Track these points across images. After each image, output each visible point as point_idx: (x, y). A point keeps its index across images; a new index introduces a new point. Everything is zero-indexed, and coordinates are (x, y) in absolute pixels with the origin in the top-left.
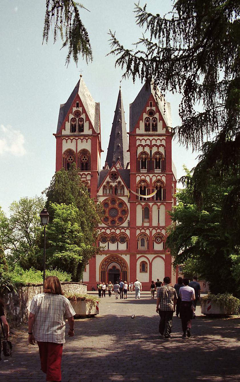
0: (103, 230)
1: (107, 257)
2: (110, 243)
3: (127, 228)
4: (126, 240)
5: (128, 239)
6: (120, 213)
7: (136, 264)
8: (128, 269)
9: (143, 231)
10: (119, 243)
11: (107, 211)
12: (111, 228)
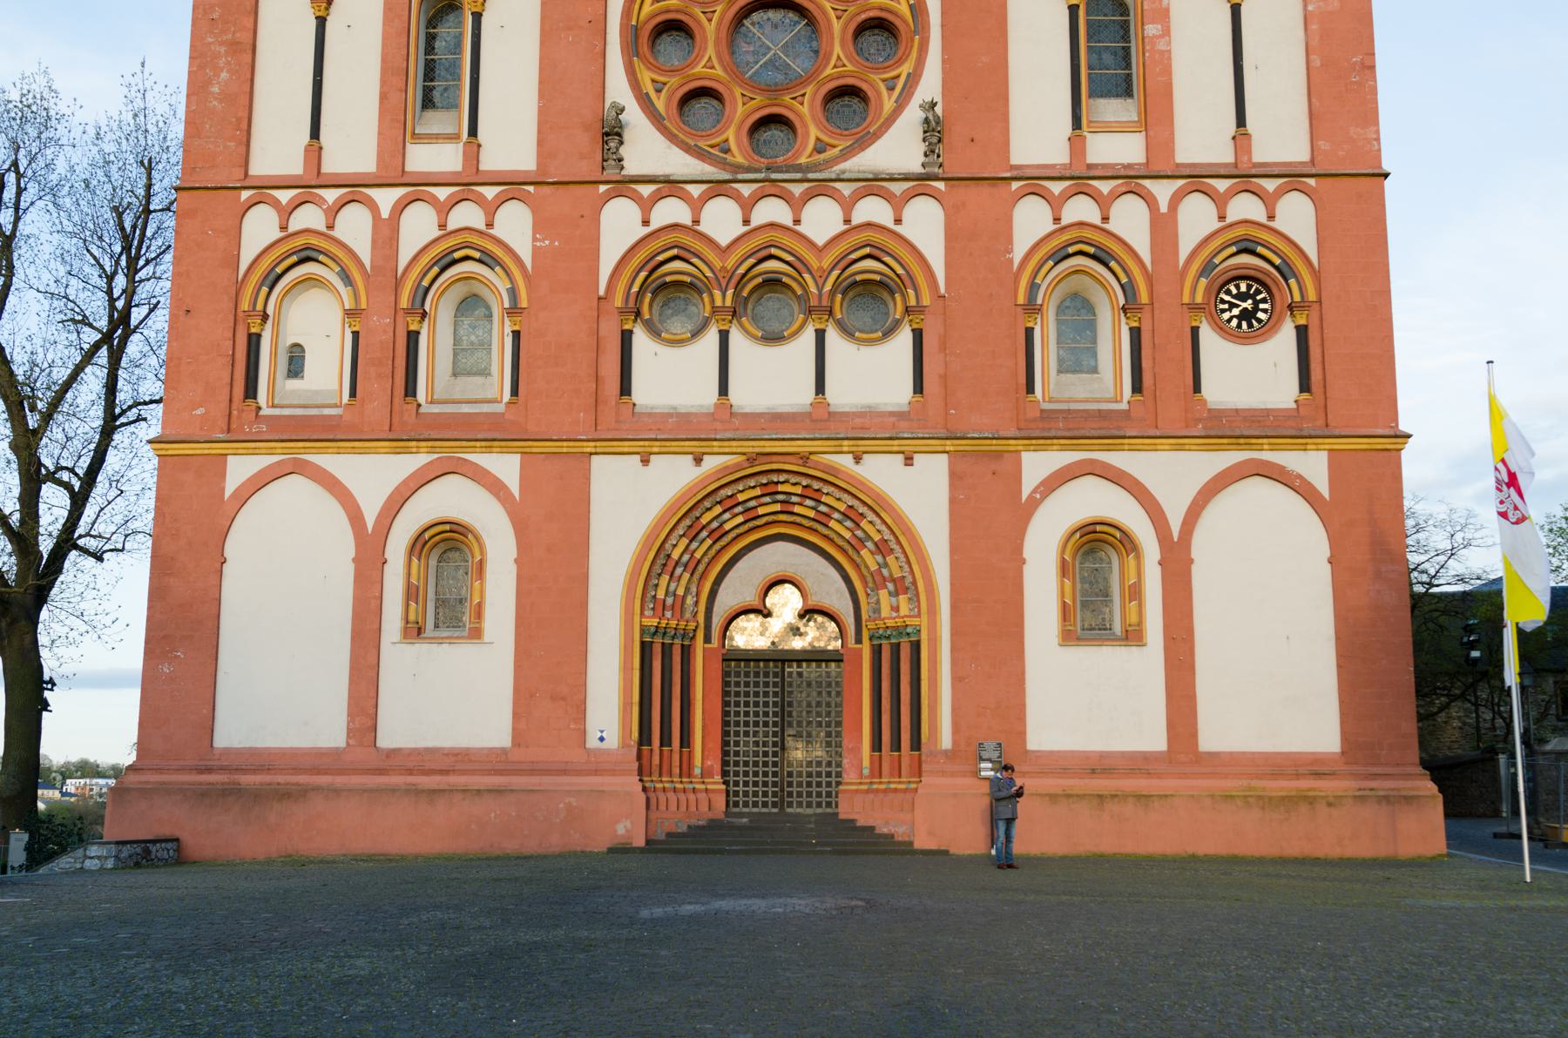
0: (671, 211)
1: (703, 482)
2: (737, 338)
3: (920, 182)
4: (907, 310)
5: (926, 301)
6: (837, 50)
7: (1018, 549)
8: (933, 611)
9: (1081, 210)
10: (833, 337)
11: (710, 28)
12: (746, 190)
